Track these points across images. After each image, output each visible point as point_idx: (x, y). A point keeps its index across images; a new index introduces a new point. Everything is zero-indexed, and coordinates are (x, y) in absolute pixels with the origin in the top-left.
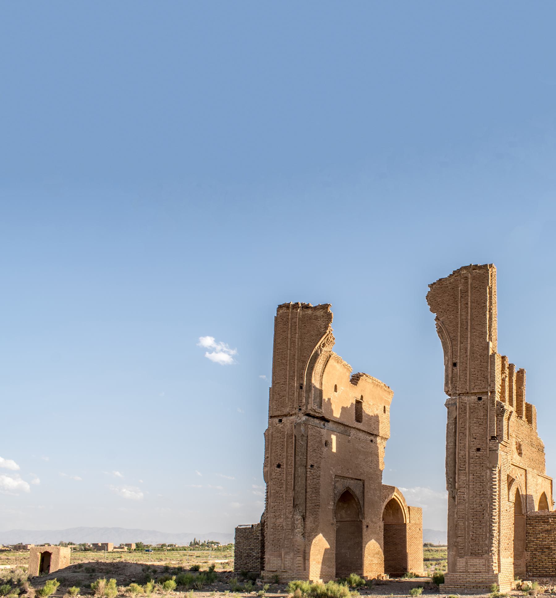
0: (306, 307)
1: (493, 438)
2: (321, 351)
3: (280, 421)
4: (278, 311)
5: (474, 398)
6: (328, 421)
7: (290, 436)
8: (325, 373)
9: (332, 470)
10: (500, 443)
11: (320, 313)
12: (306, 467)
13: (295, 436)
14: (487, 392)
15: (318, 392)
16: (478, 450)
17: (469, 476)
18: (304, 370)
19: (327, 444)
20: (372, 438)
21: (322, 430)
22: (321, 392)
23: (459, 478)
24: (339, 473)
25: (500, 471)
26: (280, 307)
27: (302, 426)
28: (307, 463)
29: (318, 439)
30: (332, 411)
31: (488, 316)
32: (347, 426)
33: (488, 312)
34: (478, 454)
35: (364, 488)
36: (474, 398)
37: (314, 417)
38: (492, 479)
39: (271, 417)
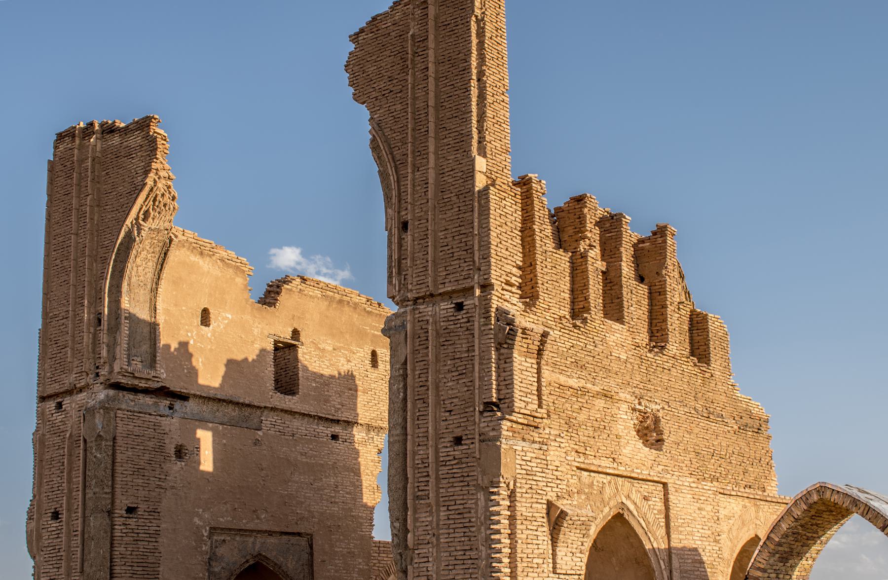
0: (109, 130)
1: (489, 406)
2: (139, 230)
3: (59, 406)
4: (56, 148)
5: (446, 306)
6: (184, 398)
7: (74, 440)
8: (163, 284)
10: (503, 418)
11: (136, 140)
12: (110, 513)
13: (85, 441)
14: (472, 288)
15: (146, 330)
16: (458, 441)
17: (438, 511)
19: (185, 452)
20: (337, 429)
21: (165, 421)
22: (153, 328)
23: (416, 520)
24: (224, 521)
25: (512, 496)
26: (61, 137)
27: (97, 415)
28: (113, 503)
29: (151, 444)
30: (193, 373)
31: (474, 92)
32: (249, 406)
33: (474, 83)
34: (458, 452)
35: (311, 554)
36: (446, 306)
37: (135, 390)
38: (489, 518)
39: (42, 399)
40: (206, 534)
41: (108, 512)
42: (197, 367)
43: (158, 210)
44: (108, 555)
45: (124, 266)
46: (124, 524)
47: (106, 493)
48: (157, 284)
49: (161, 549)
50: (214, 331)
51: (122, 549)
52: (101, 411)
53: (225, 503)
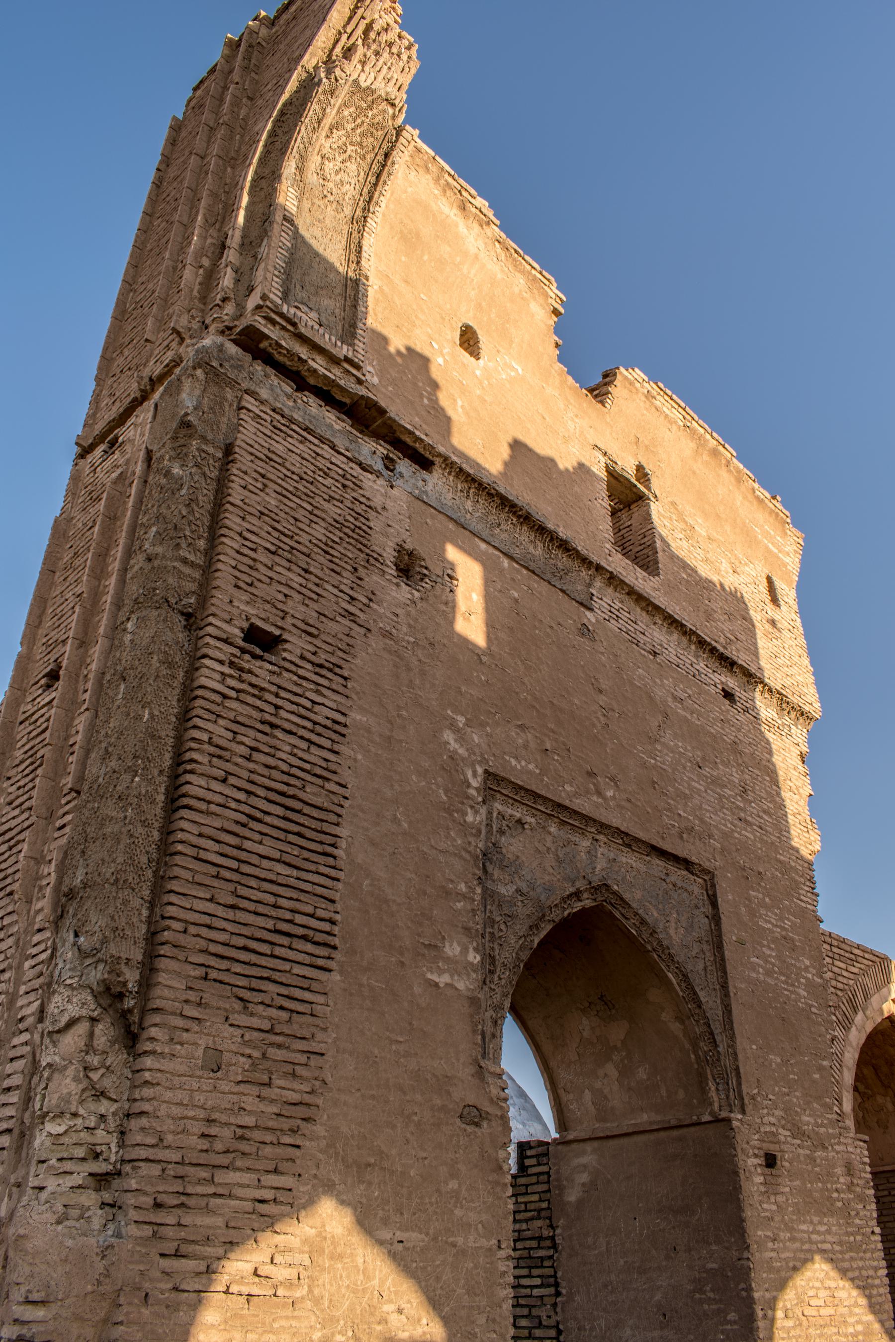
6: (423, 461)
9: (453, 727)
12: (192, 620)
18: (245, 160)
20: (732, 682)
22: (353, 291)
28: (204, 599)
29: (332, 510)
35: (716, 919)
37: (299, 379)
40: (475, 783)
41: (188, 616)
42: (450, 412)
43: (374, 47)
44: (167, 732)
45: (288, 142)
46: (232, 664)
47: (185, 561)
48: (366, 209)
49: (346, 776)
50: (485, 369)
51: (219, 730)
52: (199, 372)
53: (522, 727)
